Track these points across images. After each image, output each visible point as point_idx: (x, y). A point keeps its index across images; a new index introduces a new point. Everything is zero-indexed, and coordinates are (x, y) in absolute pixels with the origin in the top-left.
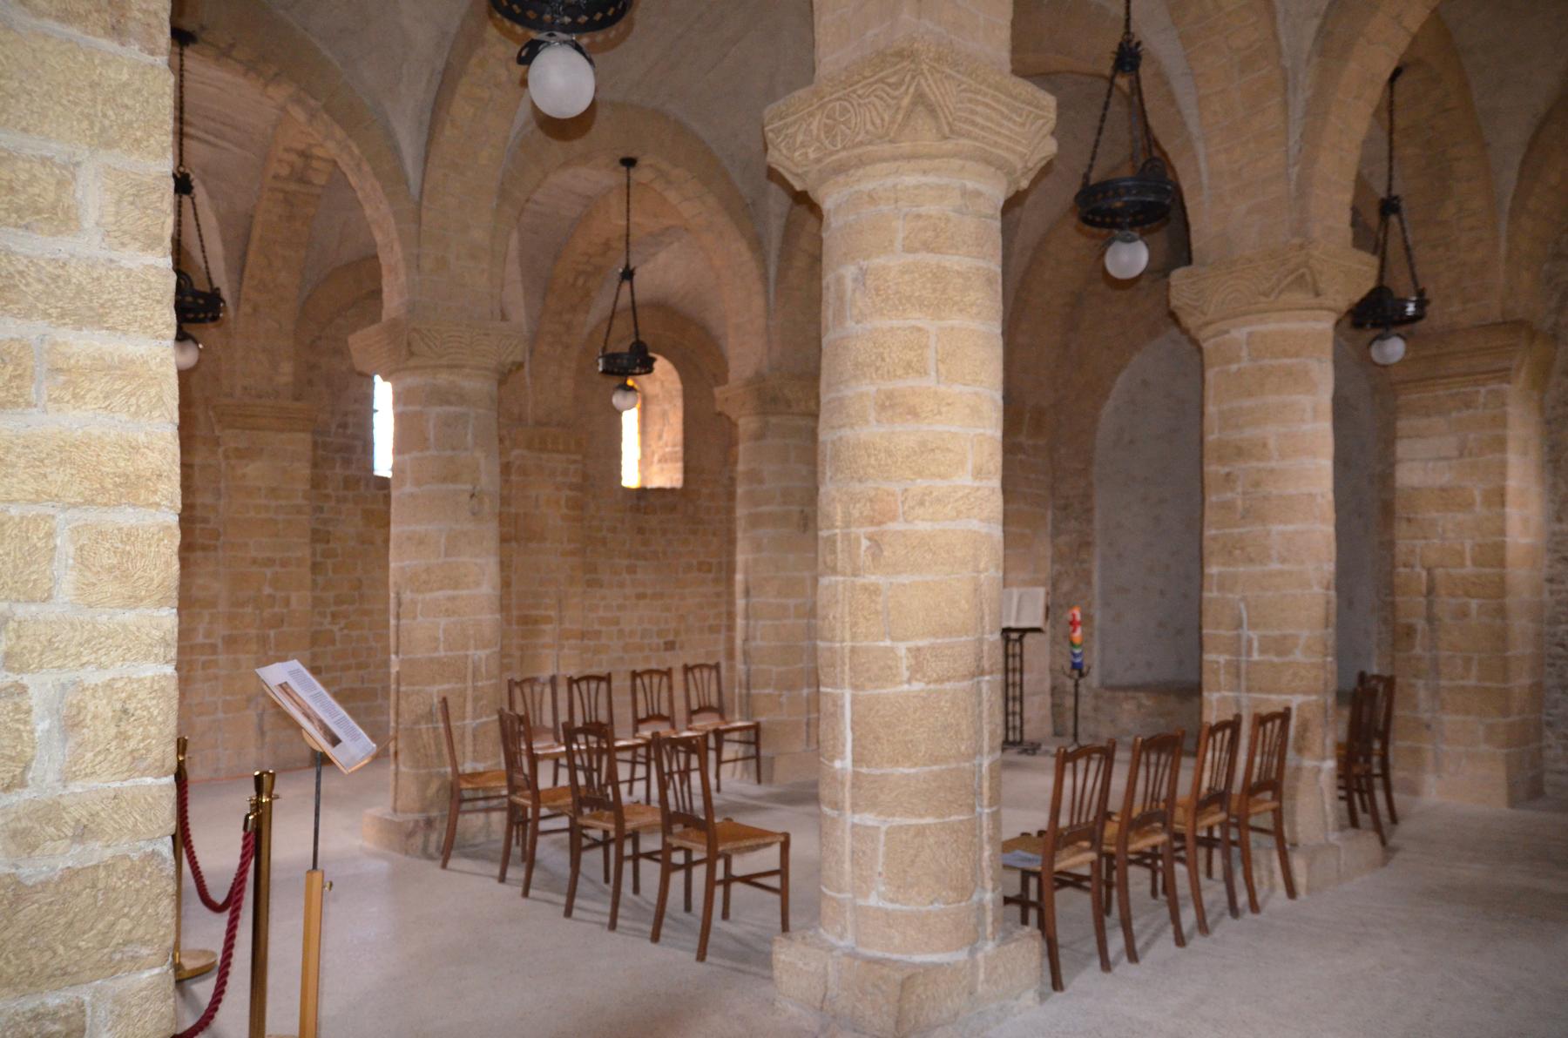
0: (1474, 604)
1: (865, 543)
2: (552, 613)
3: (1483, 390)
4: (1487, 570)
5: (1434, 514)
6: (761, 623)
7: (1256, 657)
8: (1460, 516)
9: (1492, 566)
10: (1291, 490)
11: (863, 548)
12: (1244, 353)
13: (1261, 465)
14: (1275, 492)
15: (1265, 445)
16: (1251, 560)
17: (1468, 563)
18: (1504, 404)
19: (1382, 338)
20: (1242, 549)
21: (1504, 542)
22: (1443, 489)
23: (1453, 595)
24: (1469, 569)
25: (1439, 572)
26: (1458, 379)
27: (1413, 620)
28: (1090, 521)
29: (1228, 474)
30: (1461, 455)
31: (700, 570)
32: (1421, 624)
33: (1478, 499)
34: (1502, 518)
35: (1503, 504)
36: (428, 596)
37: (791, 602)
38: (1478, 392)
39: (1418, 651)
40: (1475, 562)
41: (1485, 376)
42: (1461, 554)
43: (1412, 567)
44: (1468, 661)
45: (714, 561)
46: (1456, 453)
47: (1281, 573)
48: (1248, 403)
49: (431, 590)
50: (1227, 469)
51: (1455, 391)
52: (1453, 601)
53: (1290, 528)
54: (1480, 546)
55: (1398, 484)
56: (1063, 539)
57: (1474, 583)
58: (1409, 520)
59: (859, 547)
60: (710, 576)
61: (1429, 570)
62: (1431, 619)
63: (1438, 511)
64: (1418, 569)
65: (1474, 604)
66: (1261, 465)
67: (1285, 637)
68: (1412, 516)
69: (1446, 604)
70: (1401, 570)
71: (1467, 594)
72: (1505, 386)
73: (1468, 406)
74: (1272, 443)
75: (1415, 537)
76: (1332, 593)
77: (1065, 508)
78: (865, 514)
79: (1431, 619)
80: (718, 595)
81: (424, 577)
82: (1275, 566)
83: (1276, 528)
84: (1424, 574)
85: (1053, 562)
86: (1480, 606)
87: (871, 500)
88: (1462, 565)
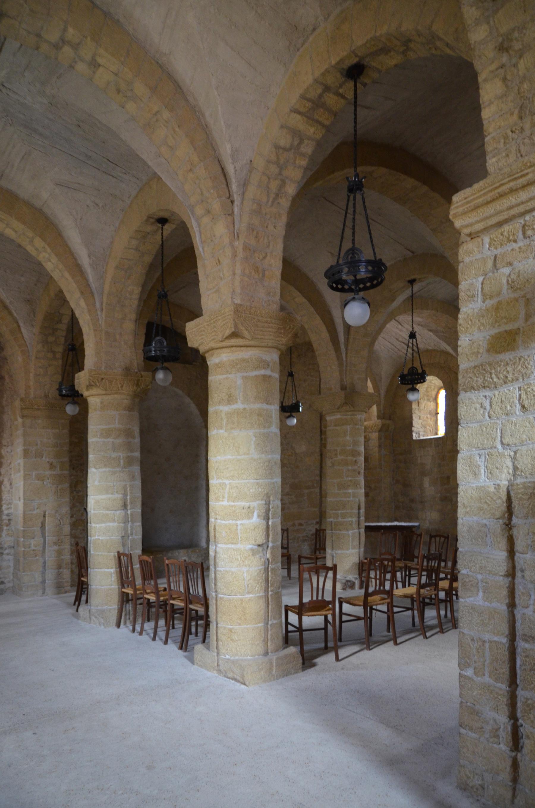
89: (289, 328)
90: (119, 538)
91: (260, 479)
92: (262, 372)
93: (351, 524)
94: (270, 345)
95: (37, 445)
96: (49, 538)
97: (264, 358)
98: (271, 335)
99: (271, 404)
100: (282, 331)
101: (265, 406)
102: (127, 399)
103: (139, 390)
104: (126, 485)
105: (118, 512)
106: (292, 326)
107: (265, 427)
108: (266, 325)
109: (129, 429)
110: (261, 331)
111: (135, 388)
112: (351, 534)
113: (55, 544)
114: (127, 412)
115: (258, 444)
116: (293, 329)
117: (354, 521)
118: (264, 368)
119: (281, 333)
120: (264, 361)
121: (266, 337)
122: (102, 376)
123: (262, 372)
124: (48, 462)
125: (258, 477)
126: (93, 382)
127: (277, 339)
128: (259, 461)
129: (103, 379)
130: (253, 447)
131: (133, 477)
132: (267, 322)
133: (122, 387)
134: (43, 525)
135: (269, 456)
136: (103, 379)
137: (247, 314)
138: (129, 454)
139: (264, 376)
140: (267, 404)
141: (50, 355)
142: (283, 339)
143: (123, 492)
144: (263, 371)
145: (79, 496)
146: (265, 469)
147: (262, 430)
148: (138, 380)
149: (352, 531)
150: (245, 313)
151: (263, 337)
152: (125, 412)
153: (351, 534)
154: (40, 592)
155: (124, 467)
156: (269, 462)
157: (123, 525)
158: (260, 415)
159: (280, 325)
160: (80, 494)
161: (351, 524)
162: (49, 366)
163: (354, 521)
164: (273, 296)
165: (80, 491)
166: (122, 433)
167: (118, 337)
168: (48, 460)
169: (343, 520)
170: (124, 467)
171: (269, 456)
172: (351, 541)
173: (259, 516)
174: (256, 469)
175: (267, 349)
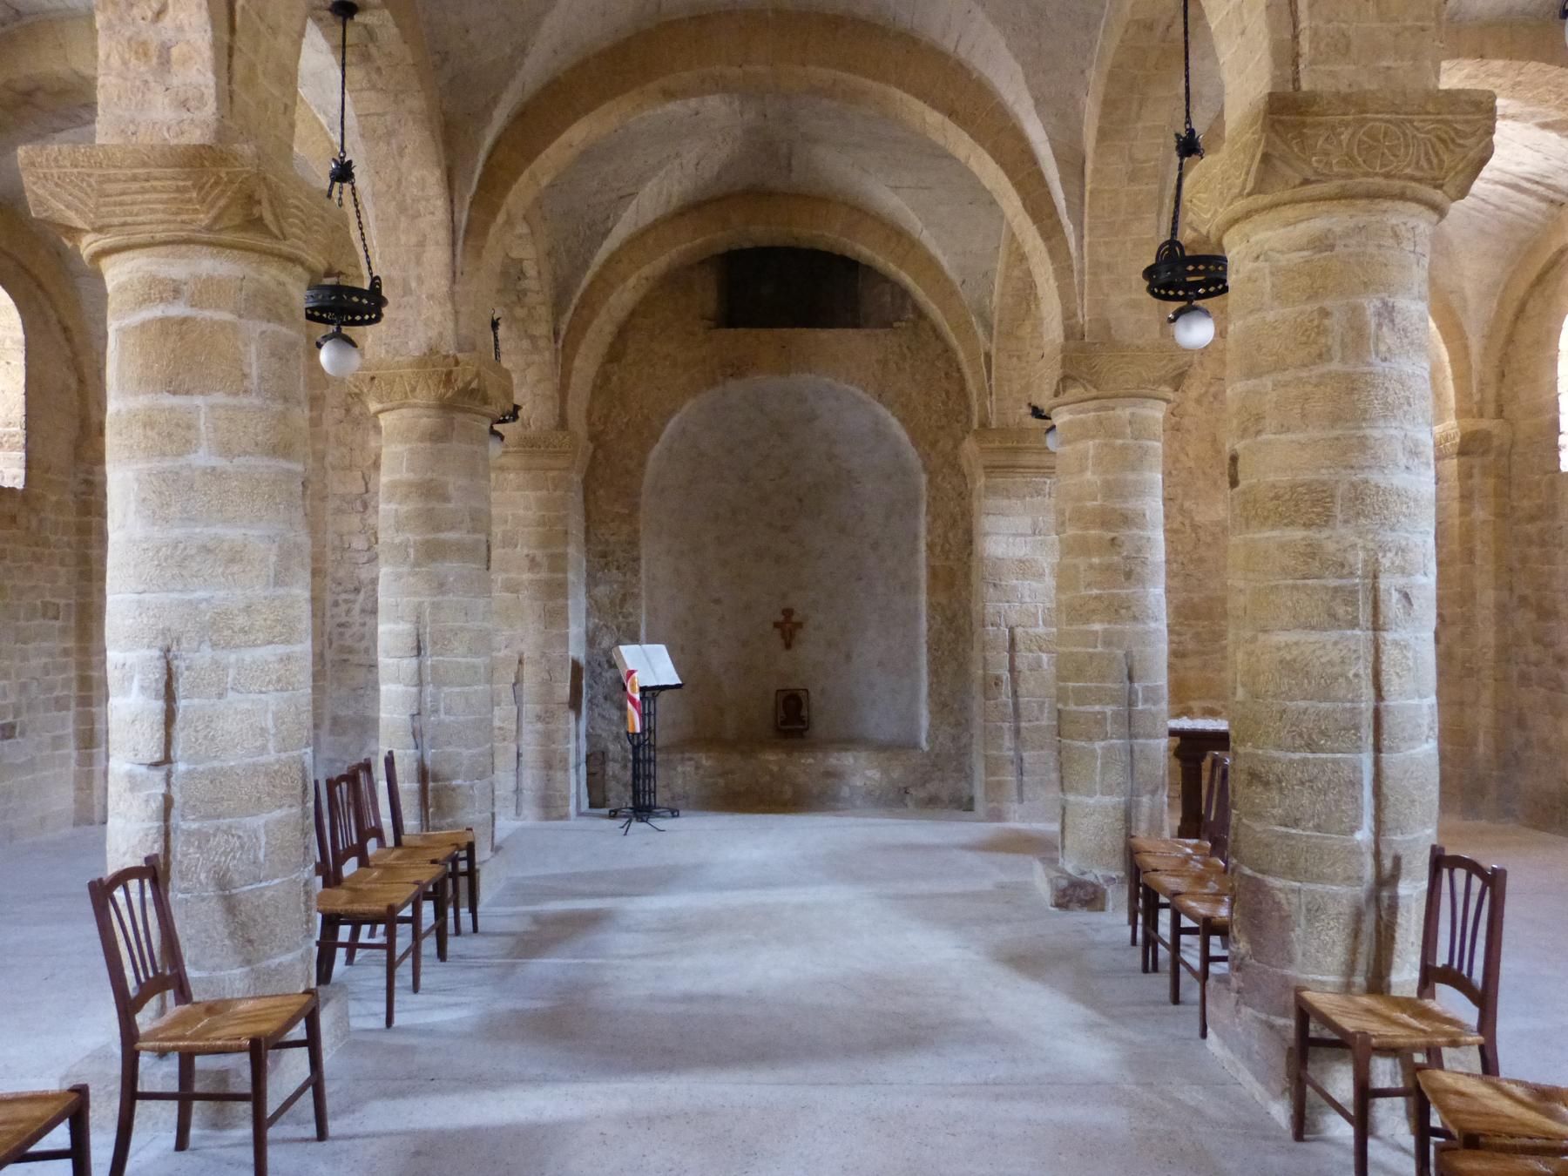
0: (1045, 657)
1: (1395, 596)
6: (446, 689)
7: (1140, 707)
8: (1034, 584)
11: (1394, 601)
12: (1128, 430)
17: (1041, 623)
20: (1128, 608)
23: (1031, 651)
24: (1041, 630)
25: (1019, 631)
27: (1000, 672)
28: (636, 572)
29: (1113, 539)
31: (44, 616)
36: (248, 655)
39: (1004, 698)
42: (1035, 615)
44: (1041, 705)
45: (62, 602)
48: (1131, 476)
49: (254, 645)
50: (1112, 535)
56: (601, 591)
58: (995, 585)
59: (1390, 600)
60: (58, 624)
61: (1011, 630)
62: (1012, 669)
65: (1045, 657)
68: (997, 582)
70: (990, 628)
71: (1040, 649)
73: (1039, 494)
75: (1000, 601)
77: (604, 555)
78: (1397, 563)
80: (66, 652)
81: (241, 621)
85: (588, 615)
87: (1403, 551)
88: (1037, 625)
89: (216, 183)
90: (406, 717)
91: (144, 592)
92: (157, 311)
93: (1100, 720)
94: (160, 236)
95: (506, 522)
96: (530, 708)
97: (162, 275)
98: (153, 211)
99: (188, 393)
100: (194, 195)
101: (168, 400)
102: (429, 417)
103: (450, 394)
104: (420, 604)
105: (406, 661)
106: (223, 175)
107: (163, 454)
108: (135, 186)
109: (431, 480)
110: (121, 204)
111: (442, 390)
112: (1099, 751)
113: (539, 718)
114: (428, 444)
115: (144, 500)
116: (231, 182)
117: (1109, 713)
118: (162, 299)
119: (190, 201)
120: (161, 282)
121: (141, 219)
122: (372, 373)
123: (157, 311)
124: (527, 556)
125: (140, 588)
126: (356, 386)
127: (179, 219)
128: (145, 546)
129: (373, 378)
130: (133, 506)
131: (441, 585)
132: (135, 178)
133: (413, 390)
134: (518, 682)
135: (177, 533)
136: (373, 378)
137: (65, 167)
138: (430, 536)
139: (164, 321)
140: (174, 393)
141: (526, 344)
142: (202, 216)
143: (414, 619)
144: (161, 306)
145: (629, 624)
146: (159, 565)
147: (156, 464)
148: (449, 374)
149: (1103, 743)
150: (59, 167)
151: (129, 219)
152: (422, 445)
153: (1099, 751)
154: (513, 811)
155: (417, 564)
156: (176, 547)
157: (415, 690)
158: (149, 424)
159: (184, 180)
160: (631, 620)
161: (1097, 722)
162: (529, 365)
163: (1109, 713)
164: (197, 108)
165: (631, 614)
166: (414, 489)
167: (414, 285)
168: (526, 551)
169: (1082, 708)
170: (417, 564)
171: (177, 533)
172: (1098, 770)
173: (142, 688)
174: (135, 566)
175: (169, 248)
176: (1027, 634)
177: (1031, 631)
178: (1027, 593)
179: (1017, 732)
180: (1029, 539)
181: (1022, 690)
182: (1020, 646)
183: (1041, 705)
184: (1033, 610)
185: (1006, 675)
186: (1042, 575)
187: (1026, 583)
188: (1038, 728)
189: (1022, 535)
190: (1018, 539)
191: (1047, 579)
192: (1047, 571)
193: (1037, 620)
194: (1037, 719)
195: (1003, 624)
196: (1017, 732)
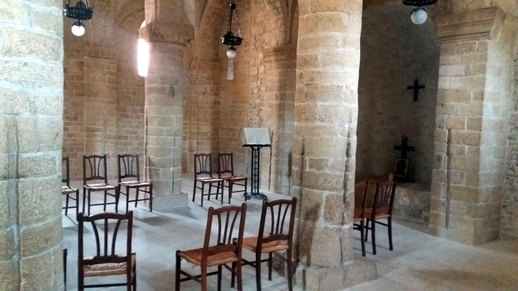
0: (467, 147)
2: (102, 127)
3: (477, 42)
4: (474, 132)
5: (453, 103)
8: (464, 104)
9: (475, 130)
10: (328, 84)
13: (314, 69)
14: (320, 84)
15: (316, 59)
16: (307, 119)
17: (466, 127)
18: (486, 49)
19: (415, 10)
21: (482, 118)
22: (458, 91)
23: (458, 143)
24: (466, 131)
25: (453, 131)
26: (467, 36)
27: (440, 154)
30: (466, 75)
32: (444, 156)
33: (472, 96)
34: (482, 106)
35: (482, 99)
37: (165, 128)
38: (475, 43)
39: (442, 168)
40: (469, 128)
41: (479, 35)
43: (442, 128)
44: (462, 175)
46: (464, 73)
47: (321, 127)
51: (465, 42)
52: (458, 145)
53: (327, 104)
54: (471, 119)
55: (439, 88)
57: (467, 137)
61: (449, 130)
62: (448, 154)
63: (454, 102)
64: (445, 129)
65: (467, 147)
66: (314, 69)
67: (321, 160)
68: (444, 103)
69: (455, 148)
70: (438, 129)
72: (488, 40)
73: (471, 50)
74: (319, 57)
76: (354, 139)
79: (448, 154)
82: (318, 123)
83: (320, 103)
84: (447, 131)
86: (469, 149)
88: (463, 129)
176: (457, 133)
177: (459, 131)
178: (459, 109)
179: (448, 189)
180: (463, 78)
181: (453, 165)
182: (453, 140)
183: (462, 175)
184: (462, 120)
185: (444, 156)
186: (469, 99)
187: (459, 103)
188: (459, 188)
189: (459, 75)
190: (457, 78)
191: (471, 101)
192: (472, 96)
193: (464, 125)
194: (459, 183)
195: (445, 127)
196: (448, 189)
